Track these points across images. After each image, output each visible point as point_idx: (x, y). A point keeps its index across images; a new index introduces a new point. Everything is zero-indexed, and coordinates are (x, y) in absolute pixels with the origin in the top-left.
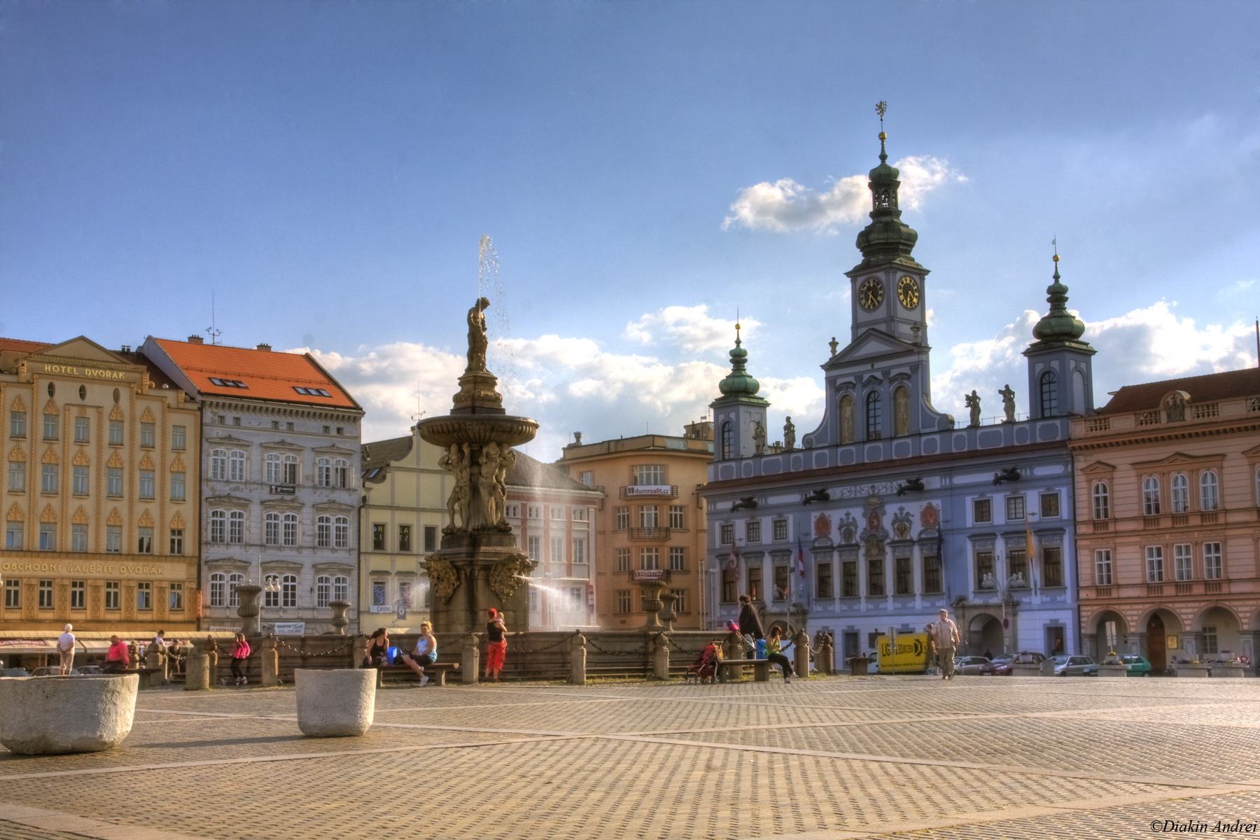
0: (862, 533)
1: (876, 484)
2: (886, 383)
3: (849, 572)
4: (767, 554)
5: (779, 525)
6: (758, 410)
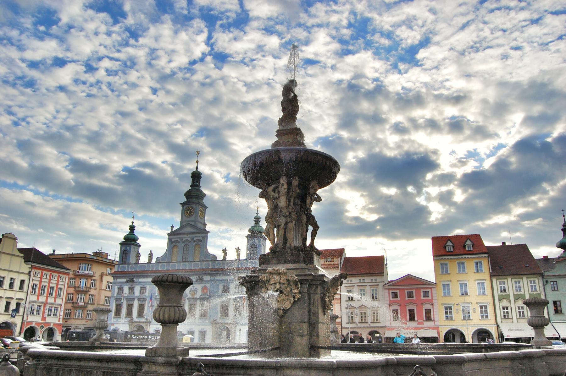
4: (136, 299)
5: (143, 289)
6: (137, 247)
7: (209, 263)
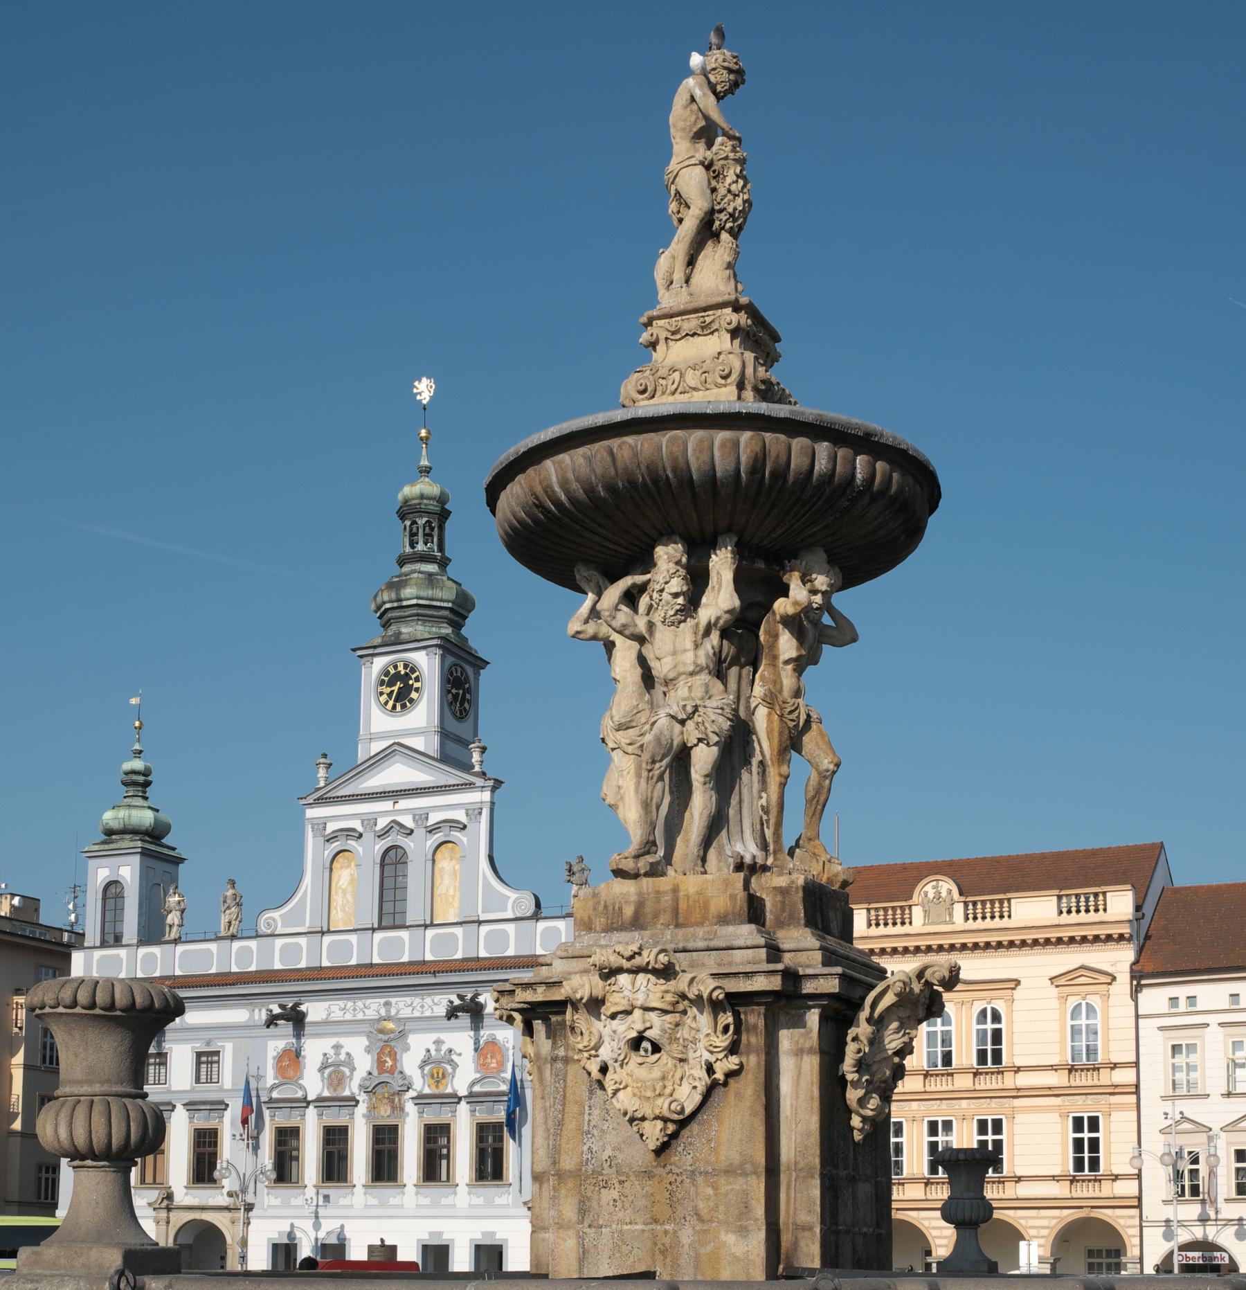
0: (364, 1079)
1: (393, 1000)
2: (420, 833)
3: (335, 1139)
4: (179, 1108)
5: (206, 1060)
7: (505, 933)
